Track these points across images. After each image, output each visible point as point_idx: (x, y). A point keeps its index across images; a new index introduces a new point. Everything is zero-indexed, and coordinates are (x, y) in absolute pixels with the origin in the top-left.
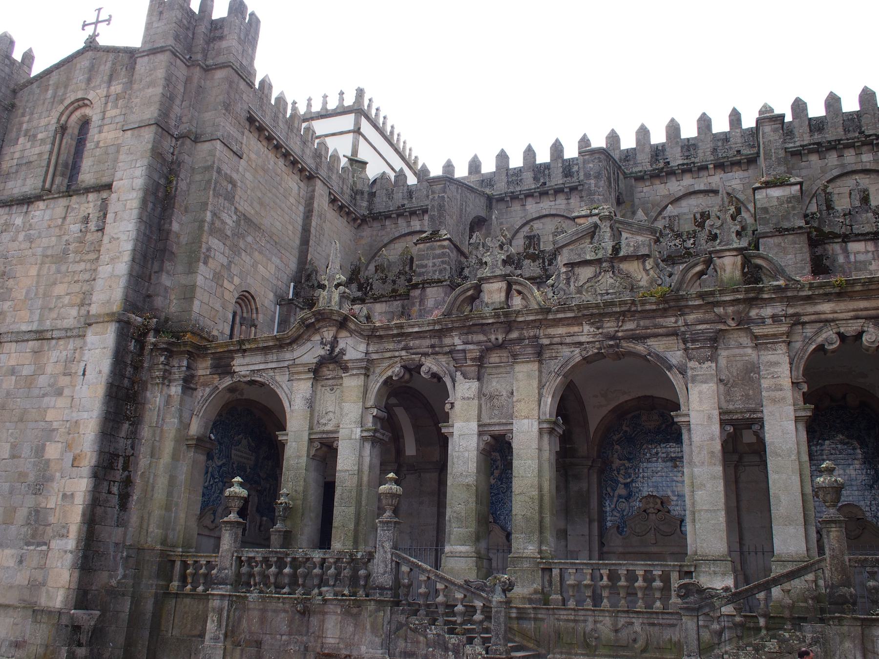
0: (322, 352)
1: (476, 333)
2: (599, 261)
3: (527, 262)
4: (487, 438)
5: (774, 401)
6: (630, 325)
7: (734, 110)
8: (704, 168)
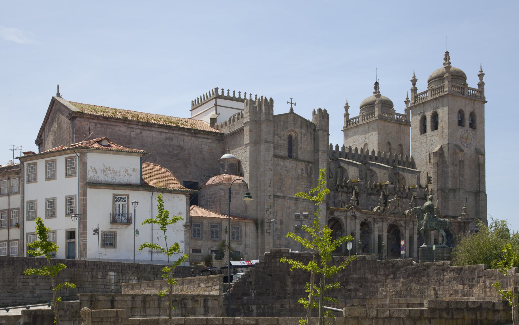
0: (352, 214)
3: (344, 188)
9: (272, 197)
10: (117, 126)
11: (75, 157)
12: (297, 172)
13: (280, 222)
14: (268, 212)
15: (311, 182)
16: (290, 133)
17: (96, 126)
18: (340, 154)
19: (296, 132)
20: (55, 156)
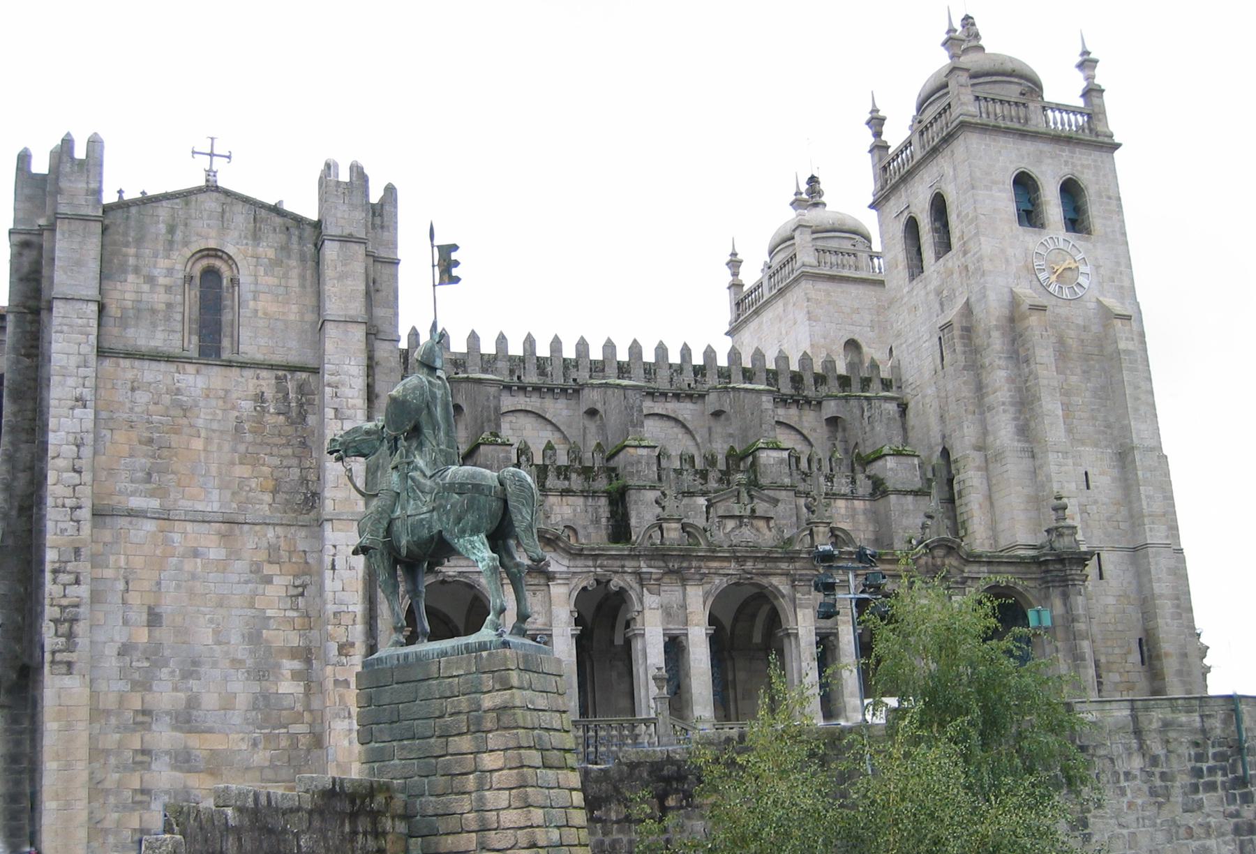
1: (658, 560)
2: (741, 517)
3: (574, 476)
4: (667, 639)
5: (844, 623)
6: (761, 566)
7: (685, 345)
8: (664, 395)
9: (85, 514)
12: (233, 408)
13: (145, 617)
14: (64, 578)
15: (303, 444)
16: (205, 263)
18: (597, 368)
19: (230, 257)
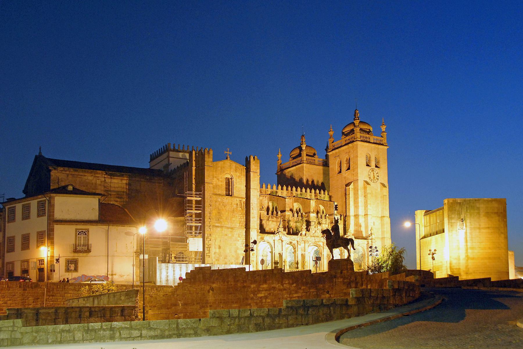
10: (85, 176)
11: (45, 201)
13: (218, 247)
14: (208, 239)
17: (68, 176)
20: (30, 200)
